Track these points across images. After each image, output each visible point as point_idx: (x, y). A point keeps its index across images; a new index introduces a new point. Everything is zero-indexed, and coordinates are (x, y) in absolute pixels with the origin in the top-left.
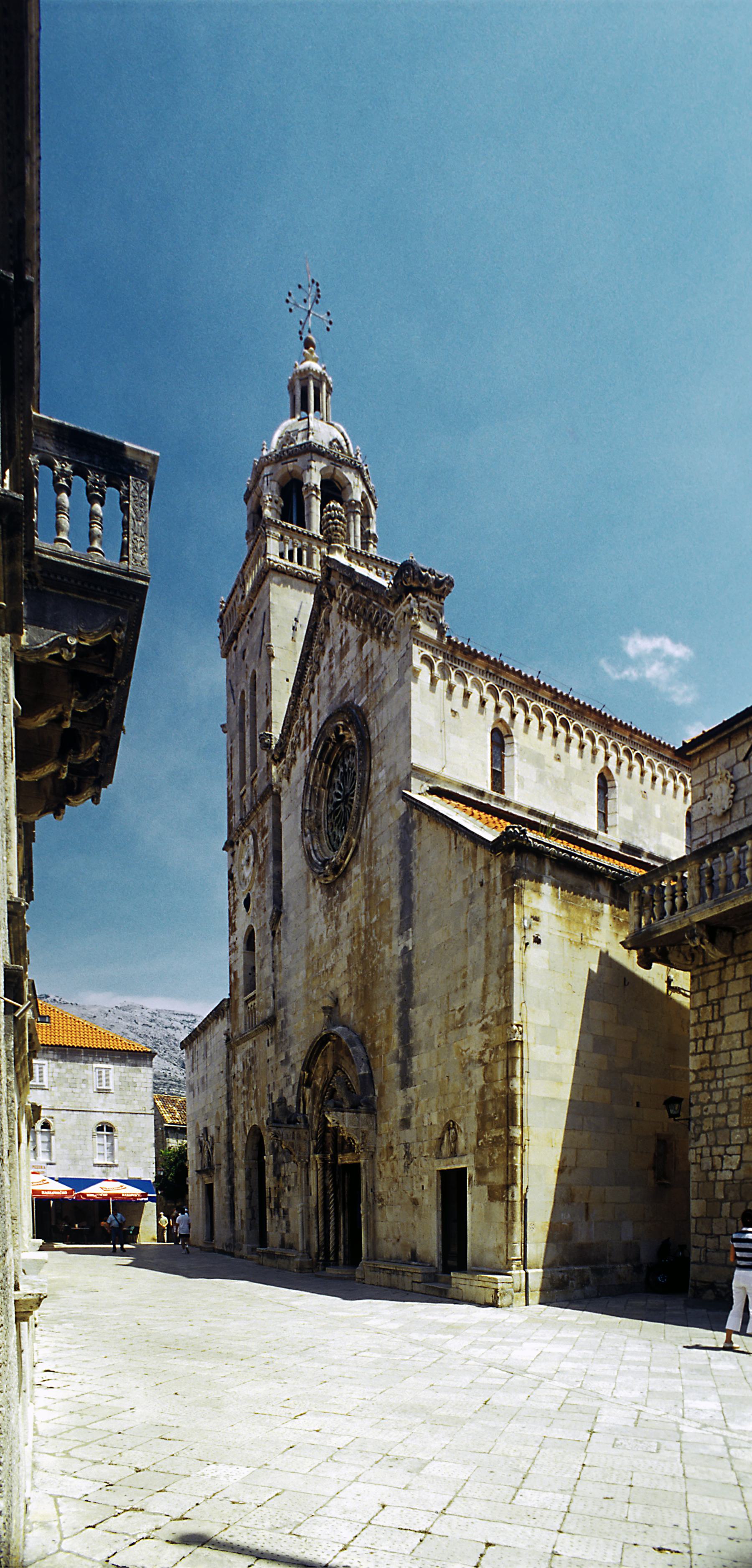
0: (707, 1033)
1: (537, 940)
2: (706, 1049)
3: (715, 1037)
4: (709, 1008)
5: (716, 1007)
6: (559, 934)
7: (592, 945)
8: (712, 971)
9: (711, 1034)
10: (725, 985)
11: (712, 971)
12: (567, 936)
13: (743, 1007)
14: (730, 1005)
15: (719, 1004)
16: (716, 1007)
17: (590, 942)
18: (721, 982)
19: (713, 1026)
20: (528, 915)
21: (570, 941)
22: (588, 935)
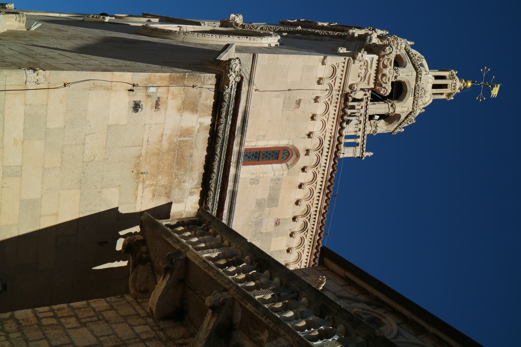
0: (63, 317)
1: (137, 107)
2: (43, 320)
3: (60, 324)
4: (92, 313)
5: (95, 318)
6: (145, 140)
7: (137, 190)
8: (134, 309)
9: (63, 320)
10: (123, 320)
11: (134, 309)
12: (144, 152)
13: (102, 339)
14: (100, 328)
15: (99, 320)
16: (95, 318)
17: (140, 186)
18: (125, 318)
19: (73, 320)
20: (161, 92)
21: (140, 156)
22: (147, 182)
